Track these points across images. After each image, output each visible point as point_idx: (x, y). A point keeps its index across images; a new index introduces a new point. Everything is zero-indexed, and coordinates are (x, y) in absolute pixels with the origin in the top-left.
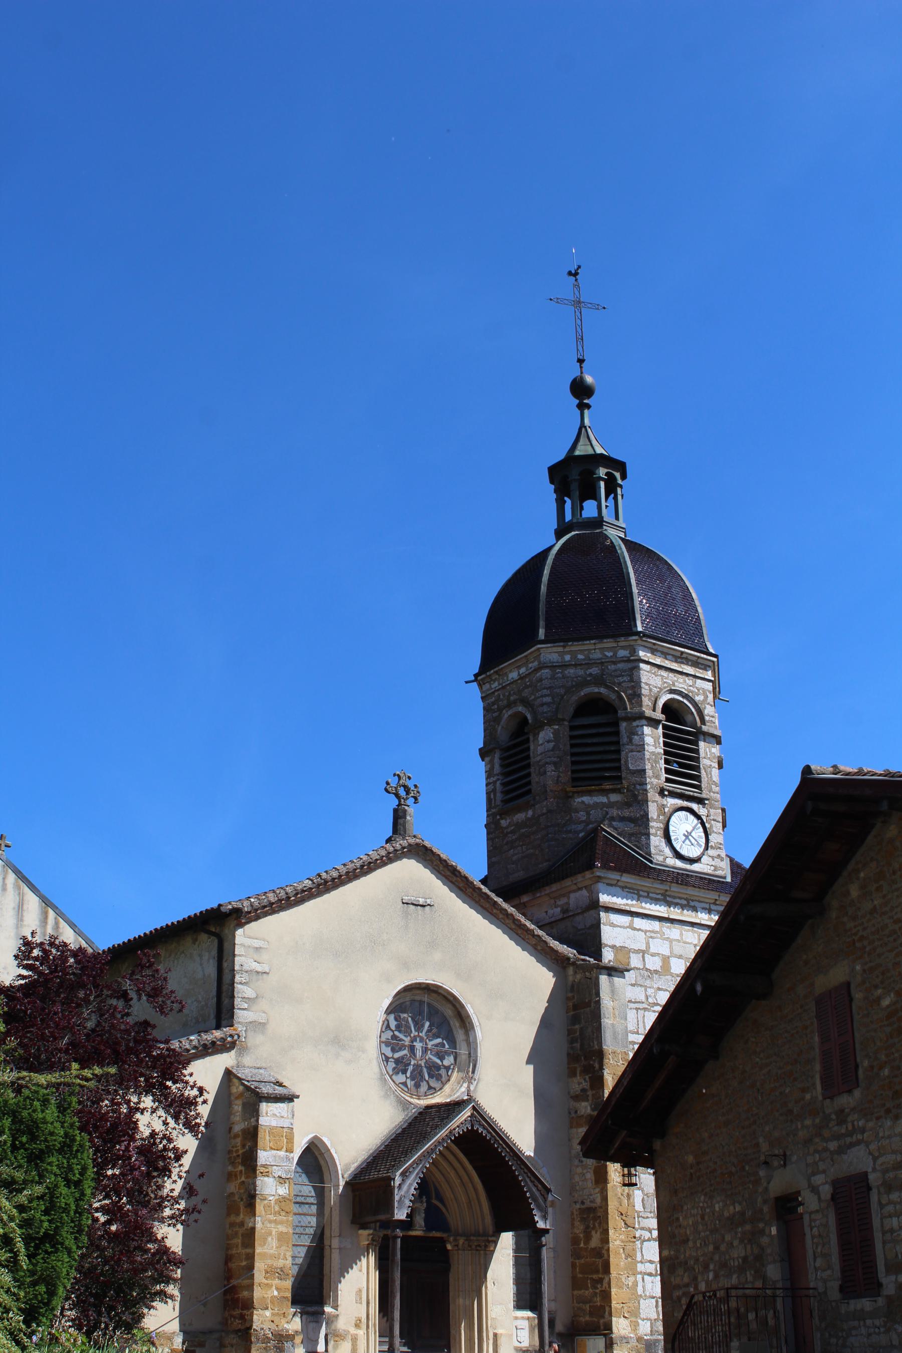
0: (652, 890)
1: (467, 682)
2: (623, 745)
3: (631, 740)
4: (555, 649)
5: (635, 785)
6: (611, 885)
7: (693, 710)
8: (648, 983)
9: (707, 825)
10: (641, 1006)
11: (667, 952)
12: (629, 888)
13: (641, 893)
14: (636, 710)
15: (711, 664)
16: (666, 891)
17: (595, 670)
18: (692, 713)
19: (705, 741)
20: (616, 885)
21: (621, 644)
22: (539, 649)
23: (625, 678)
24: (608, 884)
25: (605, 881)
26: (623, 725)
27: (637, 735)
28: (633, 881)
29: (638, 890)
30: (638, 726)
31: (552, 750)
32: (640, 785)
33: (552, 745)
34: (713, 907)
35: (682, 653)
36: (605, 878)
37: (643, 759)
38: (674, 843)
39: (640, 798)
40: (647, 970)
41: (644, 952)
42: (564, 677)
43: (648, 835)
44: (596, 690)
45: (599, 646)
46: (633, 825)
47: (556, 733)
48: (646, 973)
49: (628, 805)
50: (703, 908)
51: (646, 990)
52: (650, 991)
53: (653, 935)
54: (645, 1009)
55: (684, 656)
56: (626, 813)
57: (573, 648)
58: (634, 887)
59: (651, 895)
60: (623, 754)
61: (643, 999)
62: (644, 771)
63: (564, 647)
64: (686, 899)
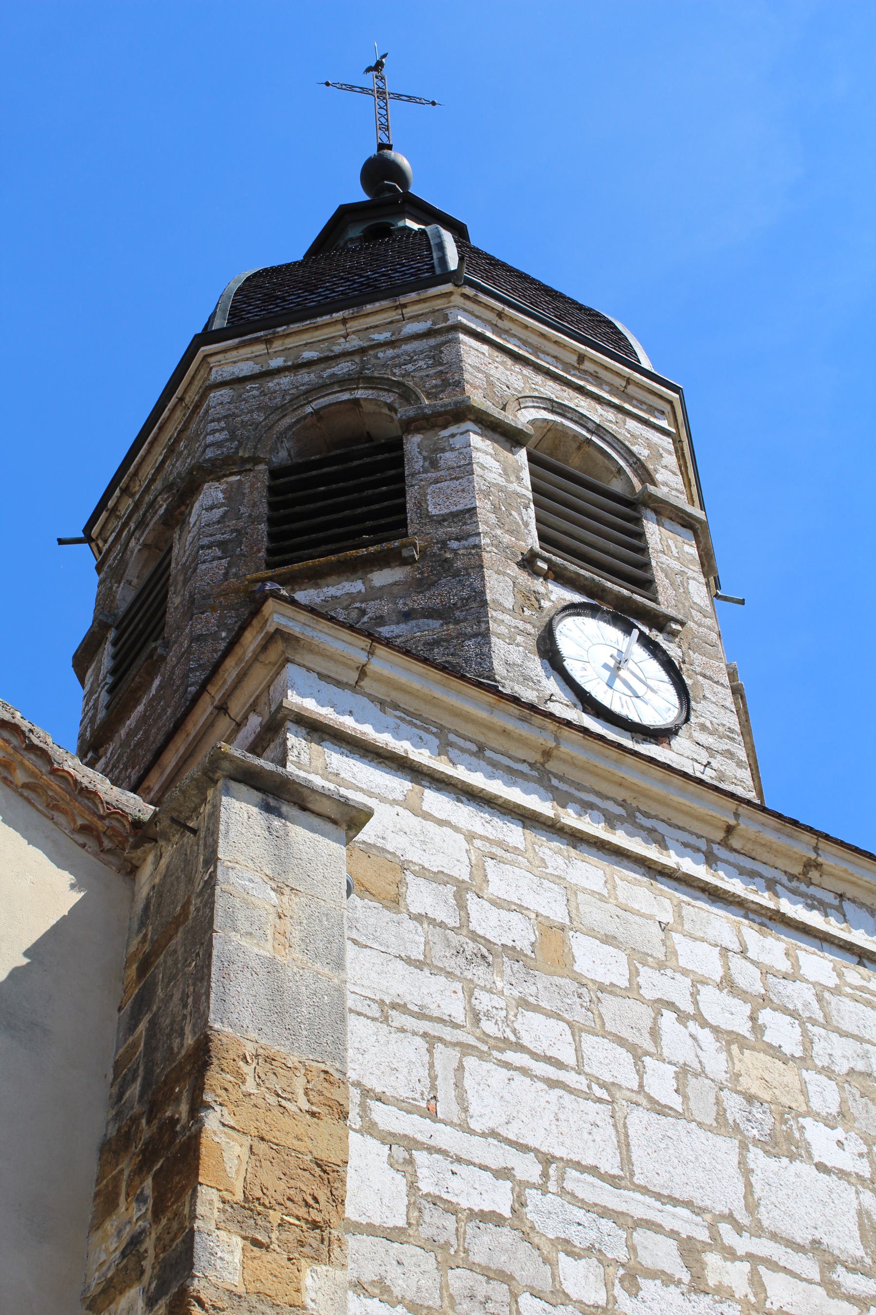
0: (494, 741)
1: (61, 542)
2: (413, 475)
3: (434, 464)
4: (245, 352)
5: (444, 544)
6: (338, 683)
7: (622, 463)
8: (479, 973)
9: (688, 682)
10: (447, 1033)
11: (558, 913)
12: (405, 711)
13: (452, 737)
14: (446, 399)
15: (667, 408)
16: (547, 754)
17: (343, 368)
18: (620, 470)
19: (659, 523)
20: (355, 688)
21: (409, 311)
22: (206, 357)
23: (421, 363)
24: (322, 676)
25: (308, 659)
26: (413, 443)
27: (452, 449)
28: (416, 684)
29: (441, 728)
30: (453, 436)
31: (219, 522)
32: (458, 539)
33: (218, 513)
34: (720, 852)
35: (581, 358)
36: (312, 649)
37: (468, 490)
38: (568, 665)
39: (458, 564)
40: (474, 936)
41: (461, 889)
42: (263, 393)
43: (485, 636)
44: (345, 396)
45: (353, 325)
46: (436, 624)
47: (233, 496)
48: (470, 947)
49: (421, 585)
50: (686, 845)
51: (470, 995)
52: (484, 1001)
53: (498, 851)
54: (466, 1049)
55: (587, 366)
56: (419, 601)
57: (290, 342)
58: (427, 712)
59: (488, 753)
60: (412, 494)
61: (456, 1009)
62: (472, 511)
63: (268, 342)
64: (623, 804)
